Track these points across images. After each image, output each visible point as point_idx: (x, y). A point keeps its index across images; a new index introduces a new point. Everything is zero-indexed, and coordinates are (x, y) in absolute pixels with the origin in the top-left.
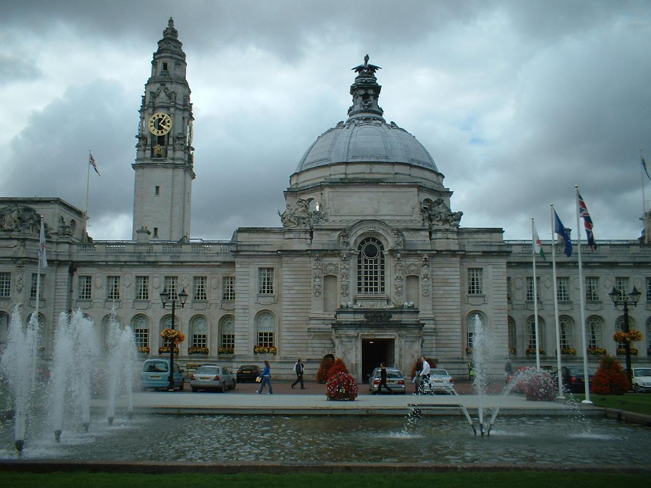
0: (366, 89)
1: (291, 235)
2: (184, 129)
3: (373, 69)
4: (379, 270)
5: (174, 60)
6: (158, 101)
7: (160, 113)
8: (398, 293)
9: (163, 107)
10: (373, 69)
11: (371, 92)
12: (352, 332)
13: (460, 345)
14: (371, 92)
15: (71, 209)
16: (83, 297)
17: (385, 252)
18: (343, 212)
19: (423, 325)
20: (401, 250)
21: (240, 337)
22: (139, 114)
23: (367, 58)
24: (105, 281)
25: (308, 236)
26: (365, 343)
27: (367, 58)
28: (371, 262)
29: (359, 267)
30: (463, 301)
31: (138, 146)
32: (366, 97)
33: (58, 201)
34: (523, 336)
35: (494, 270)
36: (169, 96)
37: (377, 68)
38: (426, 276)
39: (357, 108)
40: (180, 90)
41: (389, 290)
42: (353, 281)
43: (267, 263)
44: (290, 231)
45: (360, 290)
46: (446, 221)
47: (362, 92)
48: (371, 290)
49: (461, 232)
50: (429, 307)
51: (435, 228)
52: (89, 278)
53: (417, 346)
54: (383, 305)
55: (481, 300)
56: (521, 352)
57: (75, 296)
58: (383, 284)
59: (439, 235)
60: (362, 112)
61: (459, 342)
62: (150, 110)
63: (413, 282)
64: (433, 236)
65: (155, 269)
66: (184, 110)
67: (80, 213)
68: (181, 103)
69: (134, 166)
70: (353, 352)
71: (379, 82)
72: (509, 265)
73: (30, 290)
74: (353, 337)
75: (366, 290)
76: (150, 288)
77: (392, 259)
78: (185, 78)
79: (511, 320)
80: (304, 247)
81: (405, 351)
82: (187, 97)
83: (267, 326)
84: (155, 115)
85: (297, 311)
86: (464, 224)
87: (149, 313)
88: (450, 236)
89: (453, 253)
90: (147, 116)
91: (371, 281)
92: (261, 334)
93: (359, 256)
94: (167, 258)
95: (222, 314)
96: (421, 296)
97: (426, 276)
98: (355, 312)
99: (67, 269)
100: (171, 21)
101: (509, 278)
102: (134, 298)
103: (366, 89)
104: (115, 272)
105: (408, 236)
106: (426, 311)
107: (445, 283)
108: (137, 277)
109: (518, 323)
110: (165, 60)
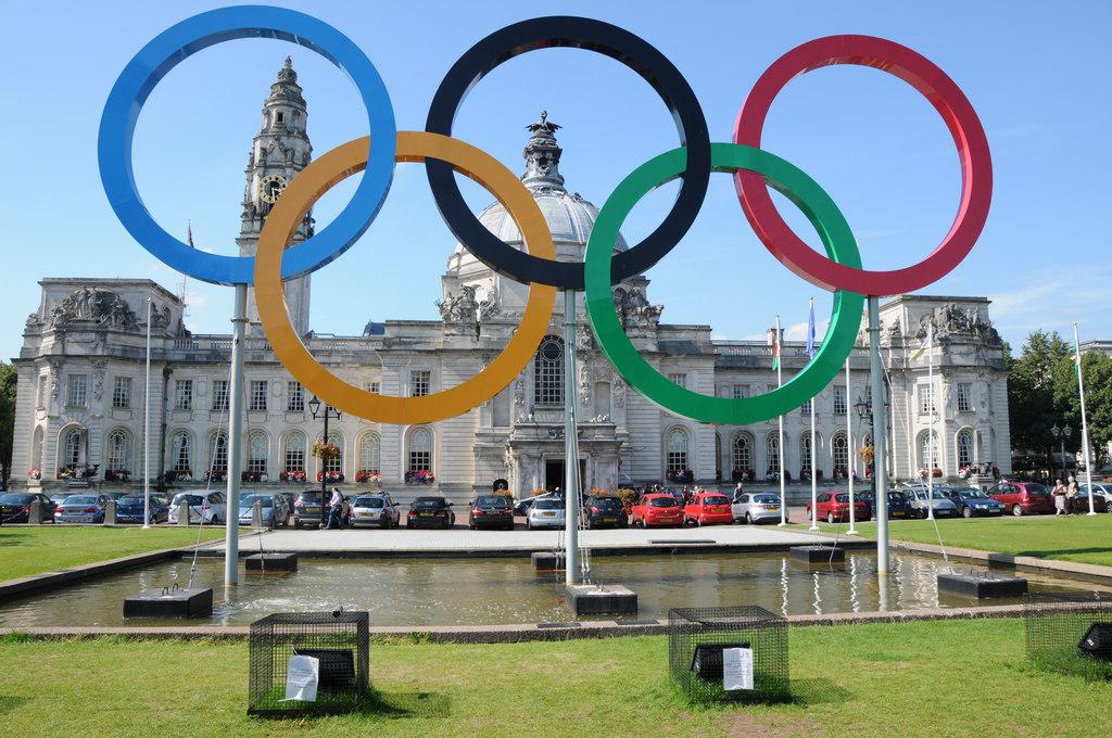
0: (544, 152)
1: (453, 331)
3: (552, 127)
5: (291, 109)
6: (269, 158)
7: (273, 174)
10: (552, 127)
11: (549, 155)
12: (534, 451)
13: (660, 468)
14: (549, 155)
15: (163, 291)
16: (293, 408)
19: (621, 442)
20: (589, 351)
21: (388, 458)
22: (245, 176)
25: (474, 331)
28: (552, 365)
29: (537, 371)
31: (245, 214)
32: (542, 162)
34: (729, 456)
35: (700, 376)
37: (556, 127)
40: (299, 145)
42: (530, 388)
43: (425, 364)
45: (537, 399)
46: (643, 315)
48: (552, 399)
49: (660, 328)
51: (631, 323)
52: (189, 383)
53: (613, 469)
56: (727, 475)
57: (171, 405)
59: (635, 332)
61: (659, 463)
62: (261, 170)
63: (604, 388)
65: (275, 372)
67: (175, 299)
68: (300, 162)
69: (238, 241)
71: (559, 144)
73: (113, 397)
74: (535, 458)
75: (546, 399)
76: (268, 396)
78: (305, 131)
80: (469, 346)
84: (267, 178)
85: (460, 425)
86: (663, 320)
87: (268, 427)
88: (648, 334)
90: (256, 178)
92: (414, 454)
93: (538, 358)
96: (612, 407)
99: (161, 371)
100: (289, 61)
109: (724, 440)
110: (280, 109)
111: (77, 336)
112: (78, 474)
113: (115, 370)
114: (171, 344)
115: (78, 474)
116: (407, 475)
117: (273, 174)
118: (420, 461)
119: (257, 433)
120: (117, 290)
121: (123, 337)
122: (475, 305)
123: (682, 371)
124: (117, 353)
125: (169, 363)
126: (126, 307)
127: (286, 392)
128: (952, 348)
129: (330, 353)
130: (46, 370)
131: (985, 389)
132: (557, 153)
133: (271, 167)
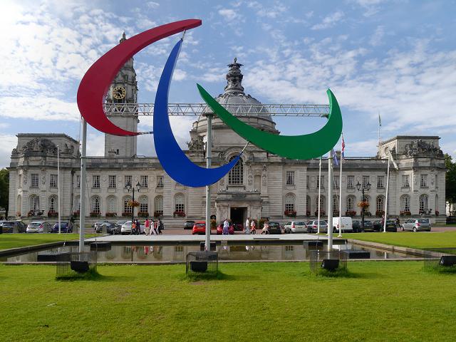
0: (235, 77)
2: (133, 96)
4: (240, 172)
7: (119, 86)
8: (250, 184)
9: (121, 83)
10: (239, 65)
11: (237, 78)
14: (237, 78)
15: (71, 139)
17: (244, 163)
18: (221, 142)
23: (236, 60)
24: (92, 178)
25: (203, 155)
26: (233, 210)
27: (236, 60)
30: (284, 188)
32: (234, 81)
33: (65, 136)
36: (124, 76)
37: (241, 65)
38: (265, 176)
39: (230, 87)
41: (245, 182)
44: (193, 152)
45: (230, 182)
47: (233, 78)
50: (266, 191)
54: (241, 190)
55: (292, 188)
58: (242, 179)
60: (233, 89)
64: (269, 155)
66: (133, 85)
67: (76, 142)
70: (226, 214)
72: (308, 169)
77: (247, 167)
79: (308, 198)
81: (253, 213)
82: (134, 78)
83: (180, 201)
89: (279, 164)
91: (236, 180)
94: (125, 166)
95: (156, 195)
97: (265, 176)
98: (227, 194)
101: (308, 176)
102: (108, 186)
103: (235, 77)
104: (97, 173)
105: (256, 155)
106: (264, 191)
107: (275, 178)
108: (110, 176)
111: (33, 158)
112: (36, 214)
113: (50, 172)
114: (74, 160)
115: (36, 214)
116: (175, 213)
117: (119, 86)
118: (180, 208)
119: (111, 197)
120: (49, 138)
121: (53, 158)
122: (203, 144)
123: (292, 170)
124: (51, 165)
125: (74, 168)
126: (54, 146)
127: (124, 180)
128: (419, 159)
129: (142, 164)
130: (21, 172)
131: (434, 177)
132: (241, 77)
133: (118, 83)
